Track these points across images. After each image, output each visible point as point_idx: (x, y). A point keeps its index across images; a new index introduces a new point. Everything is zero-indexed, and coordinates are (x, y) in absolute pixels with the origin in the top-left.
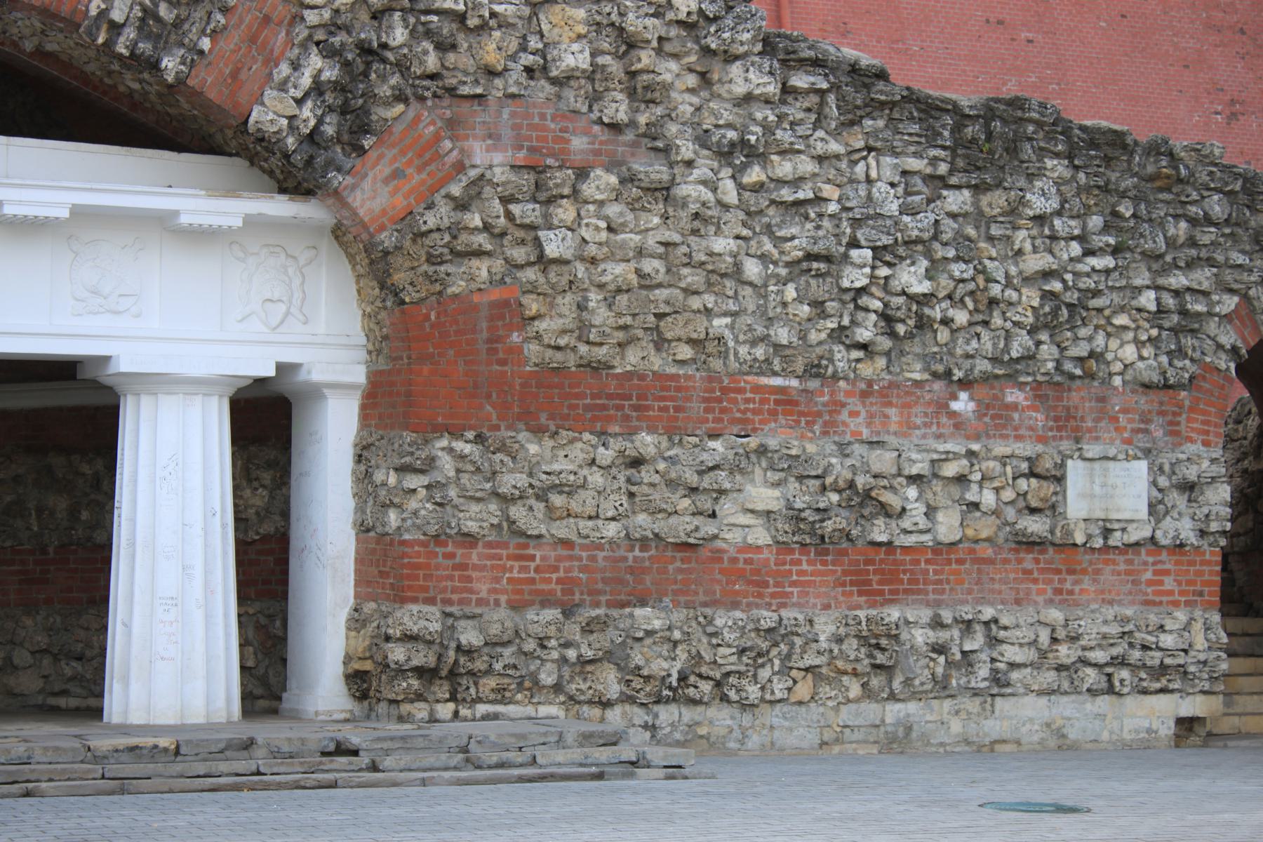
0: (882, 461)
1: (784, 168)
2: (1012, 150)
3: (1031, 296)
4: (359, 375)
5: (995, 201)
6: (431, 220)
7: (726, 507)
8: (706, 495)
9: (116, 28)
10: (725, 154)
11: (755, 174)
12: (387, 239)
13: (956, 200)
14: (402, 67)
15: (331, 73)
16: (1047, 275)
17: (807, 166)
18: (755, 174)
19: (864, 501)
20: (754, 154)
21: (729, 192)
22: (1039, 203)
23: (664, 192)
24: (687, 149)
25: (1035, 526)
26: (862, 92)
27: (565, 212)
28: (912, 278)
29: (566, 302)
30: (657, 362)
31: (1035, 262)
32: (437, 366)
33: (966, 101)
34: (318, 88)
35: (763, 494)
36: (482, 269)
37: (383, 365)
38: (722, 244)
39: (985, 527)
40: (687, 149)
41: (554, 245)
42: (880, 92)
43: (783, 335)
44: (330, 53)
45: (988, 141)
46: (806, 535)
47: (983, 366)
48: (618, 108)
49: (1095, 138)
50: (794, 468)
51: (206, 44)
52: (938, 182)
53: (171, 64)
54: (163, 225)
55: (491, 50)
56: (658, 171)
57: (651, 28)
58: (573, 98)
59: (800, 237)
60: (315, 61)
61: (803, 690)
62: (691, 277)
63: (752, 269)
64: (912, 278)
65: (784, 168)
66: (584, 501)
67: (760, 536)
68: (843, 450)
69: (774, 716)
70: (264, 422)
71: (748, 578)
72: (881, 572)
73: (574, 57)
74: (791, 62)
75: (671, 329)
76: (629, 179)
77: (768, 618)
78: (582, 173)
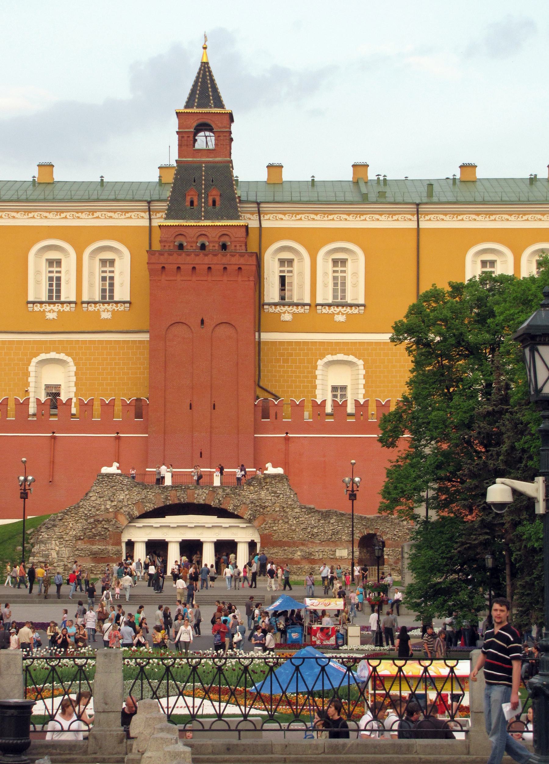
0: (313, 550)
1: (301, 519)
2: (329, 516)
3: (331, 532)
5: (327, 522)
6: (262, 526)
7: (296, 555)
8: (293, 553)
10: (294, 518)
11: (297, 520)
13: (322, 522)
14: (259, 511)
17: (303, 519)
18: (297, 520)
19: (311, 554)
20: (298, 518)
21: (295, 522)
22: (332, 522)
23: (288, 522)
24: (290, 518)
25: (332, 557)
26: (311, 511)
27: (277, 525)
28: (315, 530)
29: (277, 534)
30: (287, 540)
31: (331, 528)
32: (266, 540)
33: (324, 510)
34: (250, 514)
35: (299, 553)
36: (267, 531)
38: (293, 527)
39: (325, 557)
41: (274, 528)
42: (313, 510)
43: (301, 537)
45: (326, 515)
46: (304, 558)
47: (325, 539)
49: (341, 514)
50: (302, 551)
52: (319, 520)
53: (236, 513)
54: (239, 526)
55: (268, 509)
56: (286, 520)
57: (285, 506)
58: (278, 513)
59: (303, 526)
60: (250, 511)
61: (304, 574)
62: (290, 531)
63: (297, 530)
64: (315, 530)
65: (301, 519)
66: (279, 554)
67: (299, 558)
68: (308, 549)
69: (301, 576)
70: (252, 545)
71: (297, 562)
72: (313, 562)
73: (277, 509)
74: (302, 508)
75: (289, 536)
77: (299, 566)
78: (279, 521)
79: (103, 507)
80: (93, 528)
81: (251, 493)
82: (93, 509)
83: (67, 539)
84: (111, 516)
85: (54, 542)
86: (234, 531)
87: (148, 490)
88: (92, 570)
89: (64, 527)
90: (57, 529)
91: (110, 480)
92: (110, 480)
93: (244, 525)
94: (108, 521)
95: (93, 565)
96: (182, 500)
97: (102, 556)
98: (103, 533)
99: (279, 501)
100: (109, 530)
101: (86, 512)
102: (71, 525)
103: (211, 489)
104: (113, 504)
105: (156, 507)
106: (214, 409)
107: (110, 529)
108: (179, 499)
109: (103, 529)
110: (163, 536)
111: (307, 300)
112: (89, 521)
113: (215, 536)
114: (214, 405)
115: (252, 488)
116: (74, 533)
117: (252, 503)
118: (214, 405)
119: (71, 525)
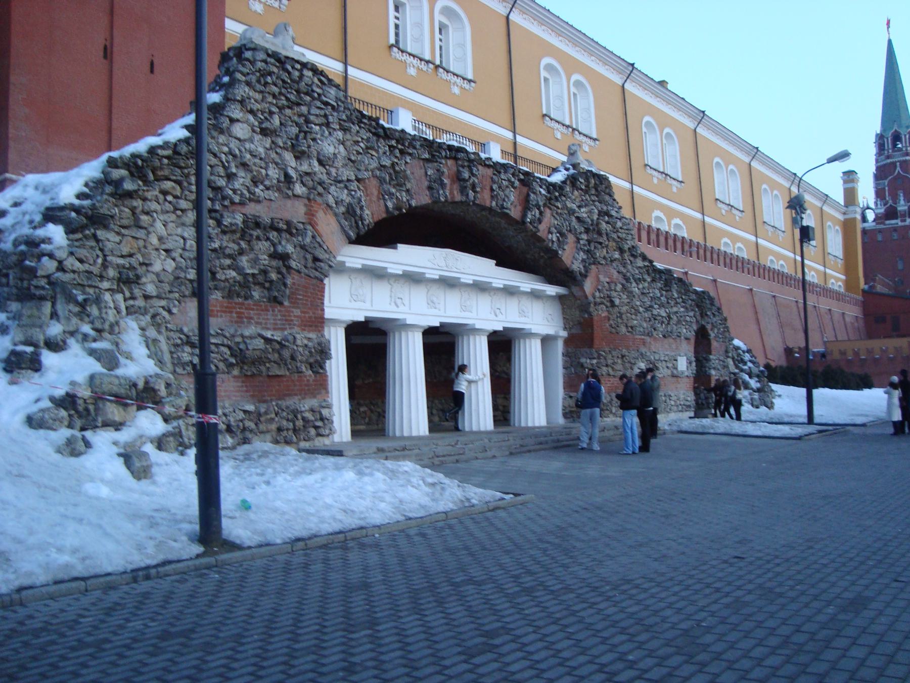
1: (646, 285)
4: (564, 334)
9: (553, 242)
11: (641, 286)
12: (591, 298)
15: (585, 257)
16: (677, 312)
24: (632, 280)
31: (675, 309)
37: (574, 331)
40: (632, 280)
44: (584, 251)
48: (622, 269)
51: (565, 247)
60: (582, 253)
63: (641, 309)
76: (623, 285)
79: (274, 173)
80: (241, 252)
81: (579, 207)
82: (241, 173)
83: (151, 289)
84: (296, 212)
85: (107, 297)
86: (527, 303)
87: (393, 143)
88: (244, 429)
89: (134, 232)
90: (109, 237)
91: (285, 76)
92: (285, 76)
93: (552, 290)
94: (290, 229)
95: (251, 408)
96: (471, 194)
97: (276, 371)
98: (274, 276)
99: (615, 236)
100: (289, 268)
101: (222, 182)
102: (159, 225)
103: (522, 177)
104: (305, 167)
105: (413, 203)
106: (152, 71)
107: (293, 264)
108: (463, 190)
109: (274, 263)
110: (394, 308)
112: (227, 221)
113: (492, 317)
114: (152, 64)
115: (576, 193)
116: (170, 265)
117: (587, 231)
118: (152, 64)
119: (159, 225)
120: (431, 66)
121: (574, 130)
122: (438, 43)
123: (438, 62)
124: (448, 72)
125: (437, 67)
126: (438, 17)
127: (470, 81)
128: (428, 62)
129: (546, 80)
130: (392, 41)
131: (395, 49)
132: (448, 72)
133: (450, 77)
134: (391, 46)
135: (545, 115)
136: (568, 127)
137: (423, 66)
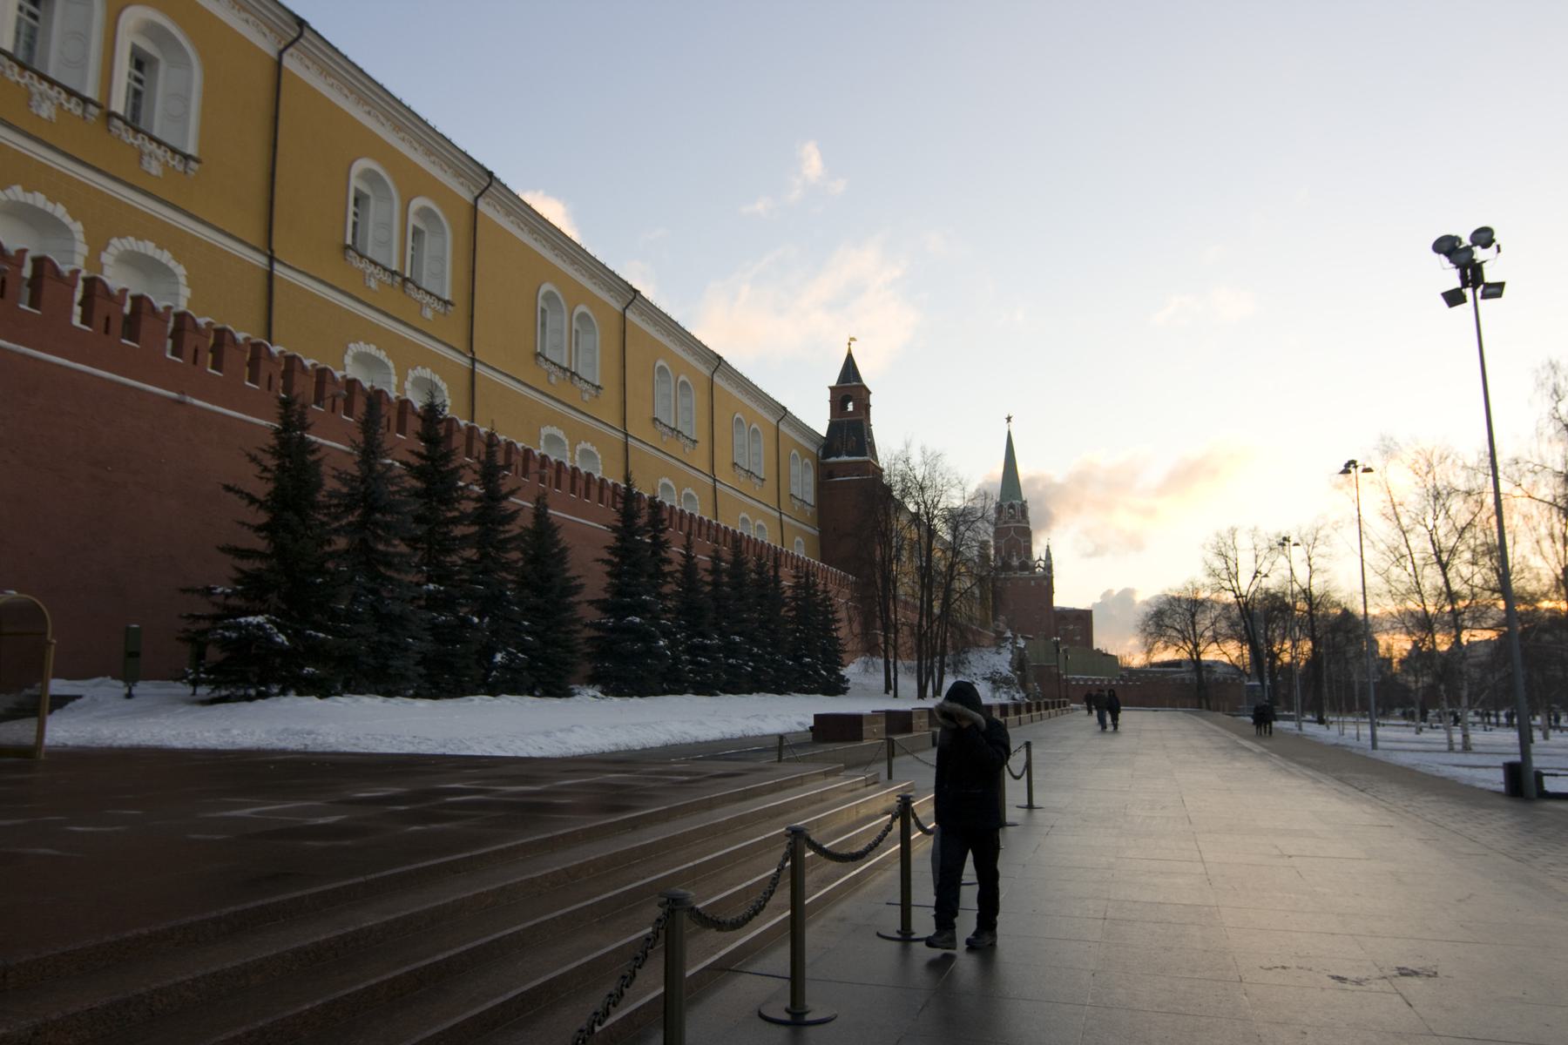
111: (90, 92)
120: (398, 279)
121: (573, 374)
122: (409, 252)
123: (408, 275)
124: (419, 288)
125: (405, 280)
126: (413, 220)
127: (446, 303)
128: (393, 273)
129: (543, 311)
130: (349, 241)
131: (351, 253)
132: (419, 288)
133: (419, 296)
134: (347, 247)
135: (538, 355)
136: (566, 370)
137: (386, 278)
